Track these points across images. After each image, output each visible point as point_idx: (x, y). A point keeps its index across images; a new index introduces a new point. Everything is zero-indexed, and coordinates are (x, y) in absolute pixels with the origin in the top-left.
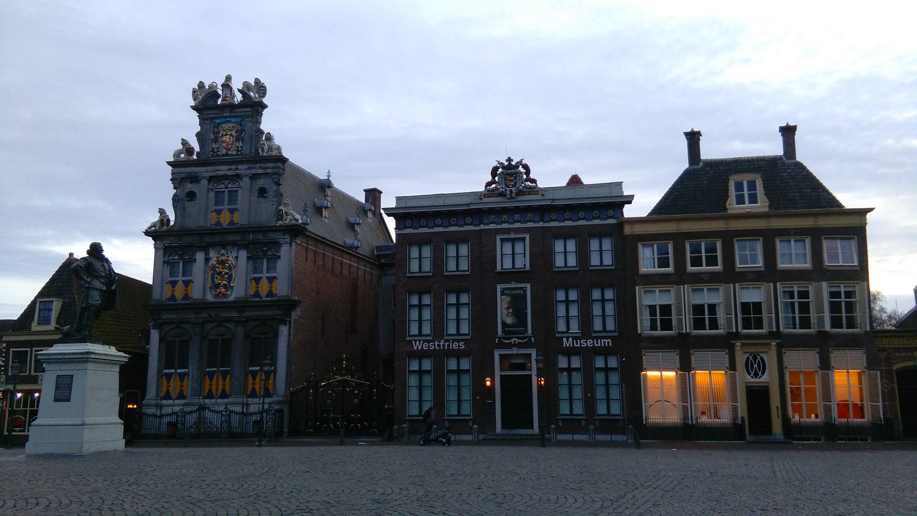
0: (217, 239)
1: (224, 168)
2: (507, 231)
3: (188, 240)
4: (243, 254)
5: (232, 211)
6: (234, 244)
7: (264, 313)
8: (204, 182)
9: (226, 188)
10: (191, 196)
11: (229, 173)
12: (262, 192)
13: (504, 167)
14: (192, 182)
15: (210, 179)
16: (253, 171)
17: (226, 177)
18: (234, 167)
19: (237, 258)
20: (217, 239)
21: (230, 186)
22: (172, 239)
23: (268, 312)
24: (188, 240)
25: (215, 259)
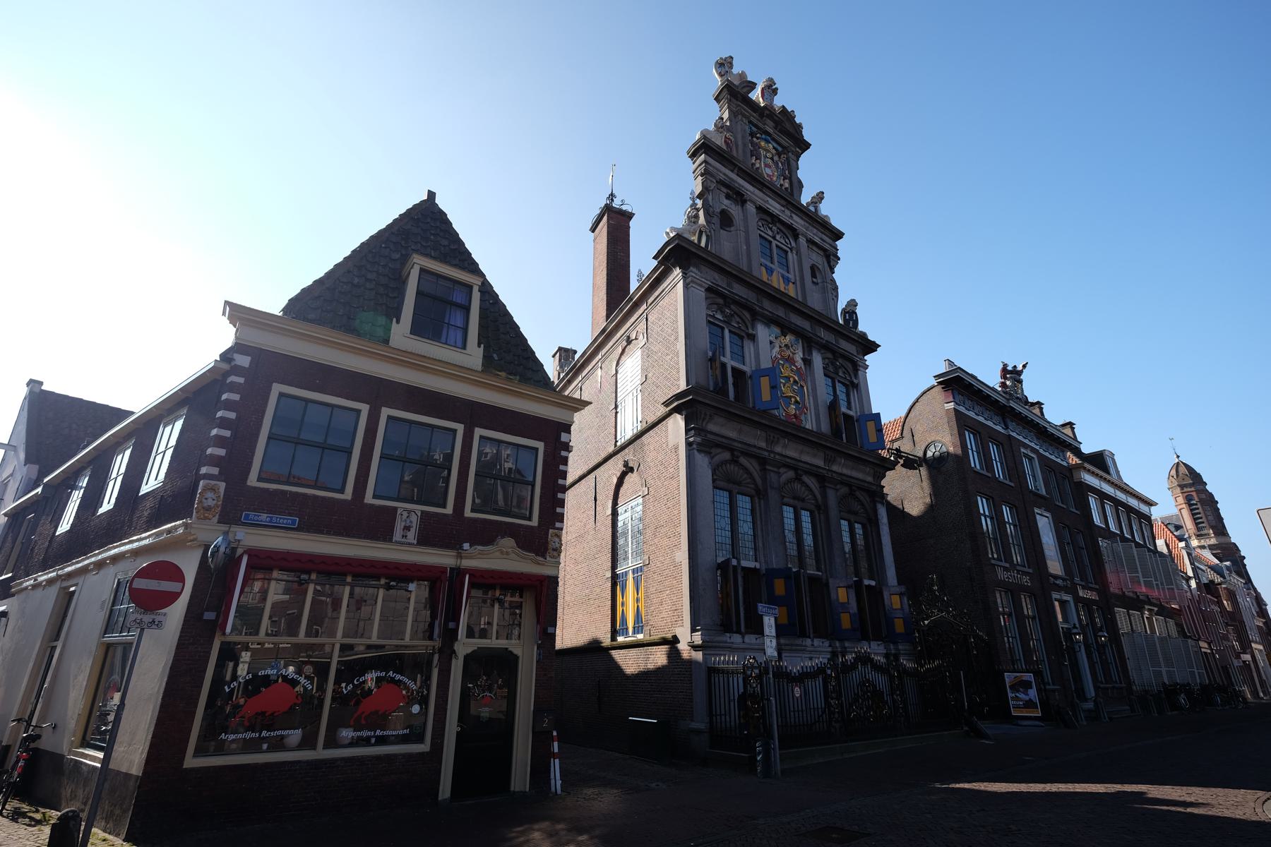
0: (781, 312)
1: (778, 206)
2: (1026, 446)
3: (739, 290)
4: (818, 360)
5: (787, 280)
6: (799, 334)
7: (855, 474)
8: (751, 208)
9: (774, 238)
10: (725, 220)
11: (784, 217)
12: (814, 269)
13: (1011, 372)
14: (728, 197)
15: (760, 209)
16: (810, 235)
17: (774, 219)
18: (788, 212)
19: (808, 362)
20: (781, 312)
21: (778, 237)
22: (716, 276)
23: (860, 476)
24: (739, 290)
25: (777, 349)
